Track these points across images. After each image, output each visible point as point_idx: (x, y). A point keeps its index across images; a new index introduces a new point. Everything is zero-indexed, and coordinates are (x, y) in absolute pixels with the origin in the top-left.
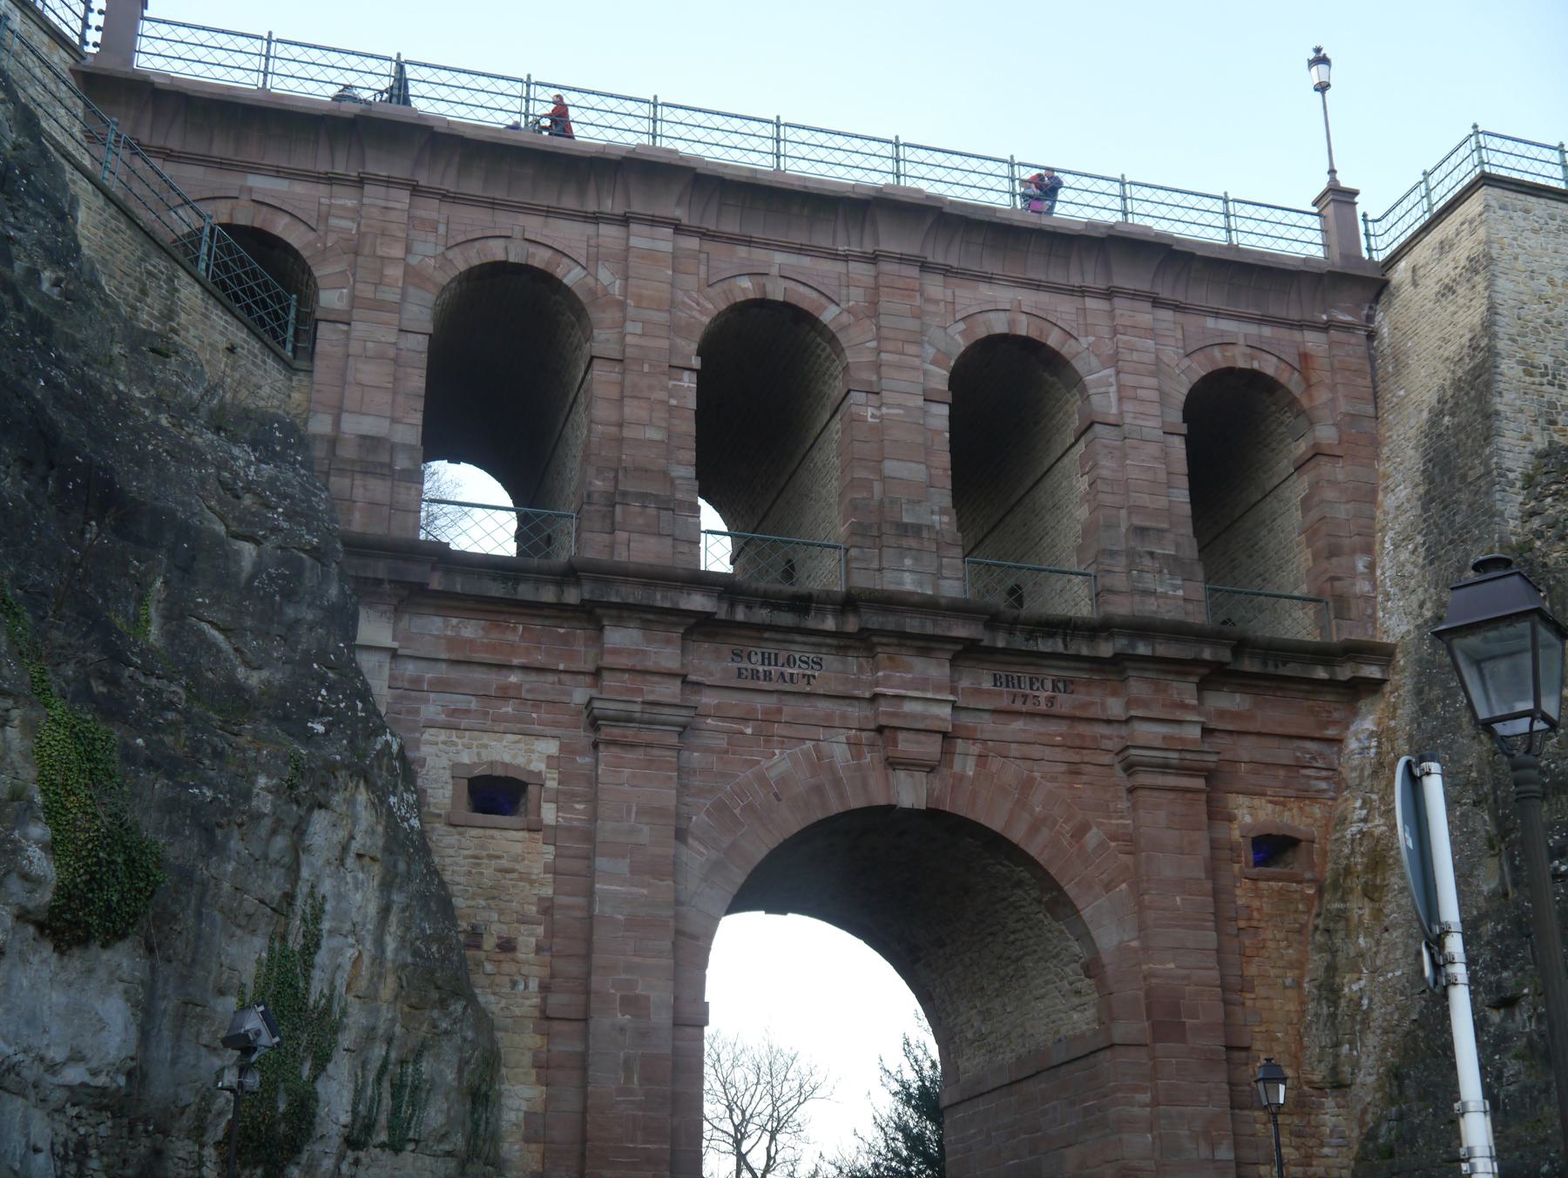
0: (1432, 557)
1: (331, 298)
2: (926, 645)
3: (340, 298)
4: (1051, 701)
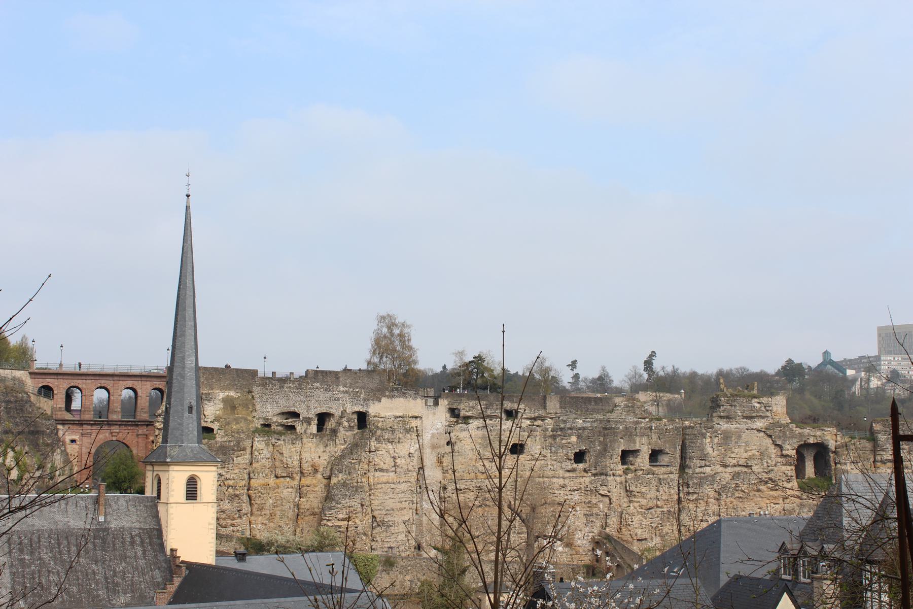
1: (55, 392)
2: (116, 425)
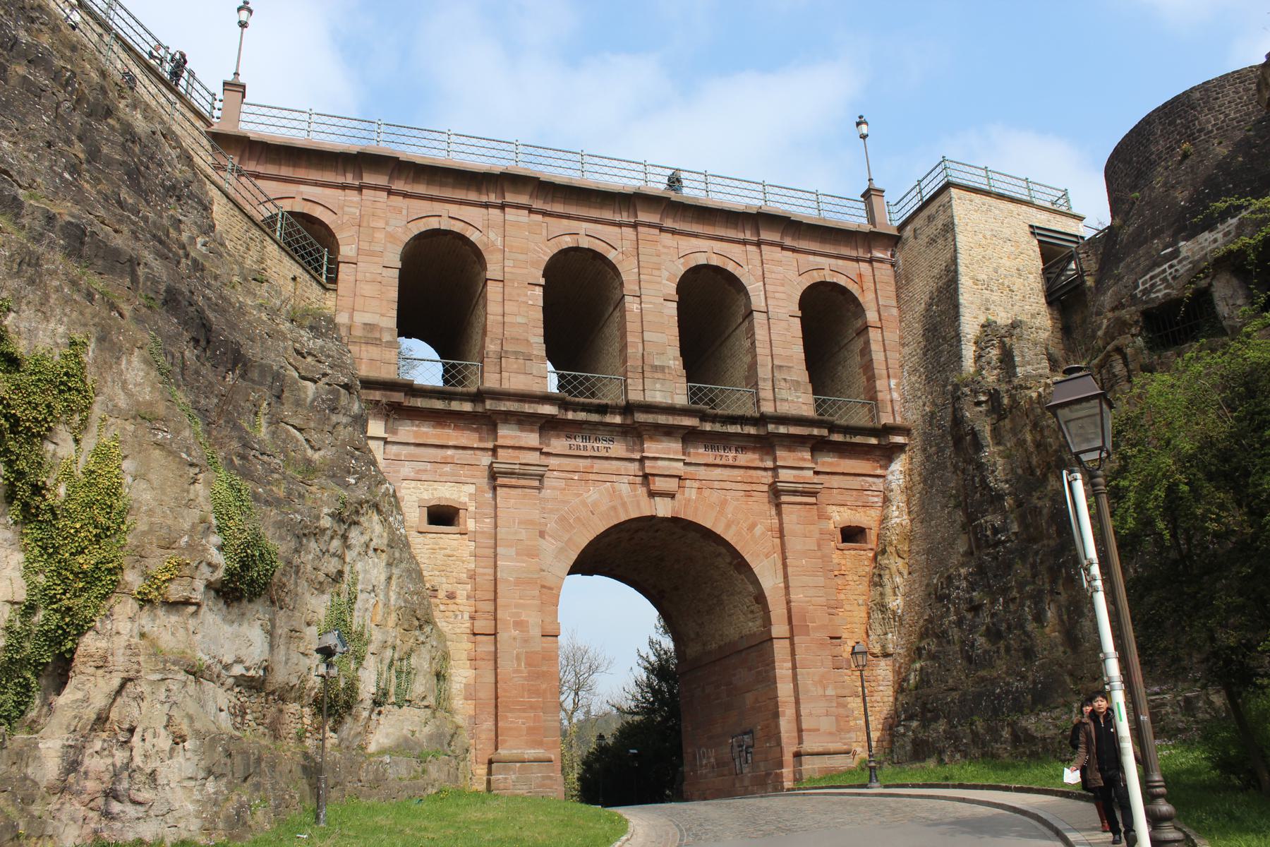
0: (929, 380)
1: (346, 251)
2: (668, 432)
3: (351, 250)
4: (735, 458)
